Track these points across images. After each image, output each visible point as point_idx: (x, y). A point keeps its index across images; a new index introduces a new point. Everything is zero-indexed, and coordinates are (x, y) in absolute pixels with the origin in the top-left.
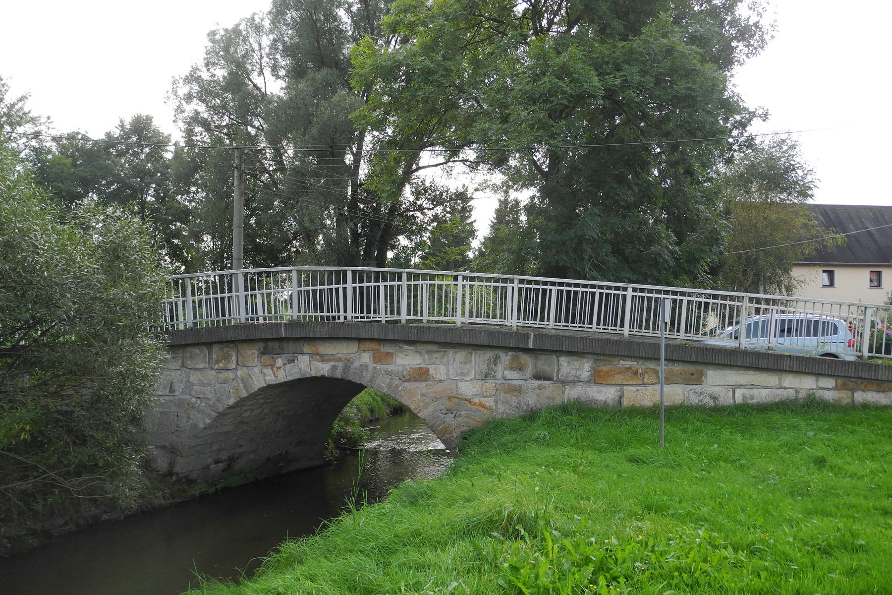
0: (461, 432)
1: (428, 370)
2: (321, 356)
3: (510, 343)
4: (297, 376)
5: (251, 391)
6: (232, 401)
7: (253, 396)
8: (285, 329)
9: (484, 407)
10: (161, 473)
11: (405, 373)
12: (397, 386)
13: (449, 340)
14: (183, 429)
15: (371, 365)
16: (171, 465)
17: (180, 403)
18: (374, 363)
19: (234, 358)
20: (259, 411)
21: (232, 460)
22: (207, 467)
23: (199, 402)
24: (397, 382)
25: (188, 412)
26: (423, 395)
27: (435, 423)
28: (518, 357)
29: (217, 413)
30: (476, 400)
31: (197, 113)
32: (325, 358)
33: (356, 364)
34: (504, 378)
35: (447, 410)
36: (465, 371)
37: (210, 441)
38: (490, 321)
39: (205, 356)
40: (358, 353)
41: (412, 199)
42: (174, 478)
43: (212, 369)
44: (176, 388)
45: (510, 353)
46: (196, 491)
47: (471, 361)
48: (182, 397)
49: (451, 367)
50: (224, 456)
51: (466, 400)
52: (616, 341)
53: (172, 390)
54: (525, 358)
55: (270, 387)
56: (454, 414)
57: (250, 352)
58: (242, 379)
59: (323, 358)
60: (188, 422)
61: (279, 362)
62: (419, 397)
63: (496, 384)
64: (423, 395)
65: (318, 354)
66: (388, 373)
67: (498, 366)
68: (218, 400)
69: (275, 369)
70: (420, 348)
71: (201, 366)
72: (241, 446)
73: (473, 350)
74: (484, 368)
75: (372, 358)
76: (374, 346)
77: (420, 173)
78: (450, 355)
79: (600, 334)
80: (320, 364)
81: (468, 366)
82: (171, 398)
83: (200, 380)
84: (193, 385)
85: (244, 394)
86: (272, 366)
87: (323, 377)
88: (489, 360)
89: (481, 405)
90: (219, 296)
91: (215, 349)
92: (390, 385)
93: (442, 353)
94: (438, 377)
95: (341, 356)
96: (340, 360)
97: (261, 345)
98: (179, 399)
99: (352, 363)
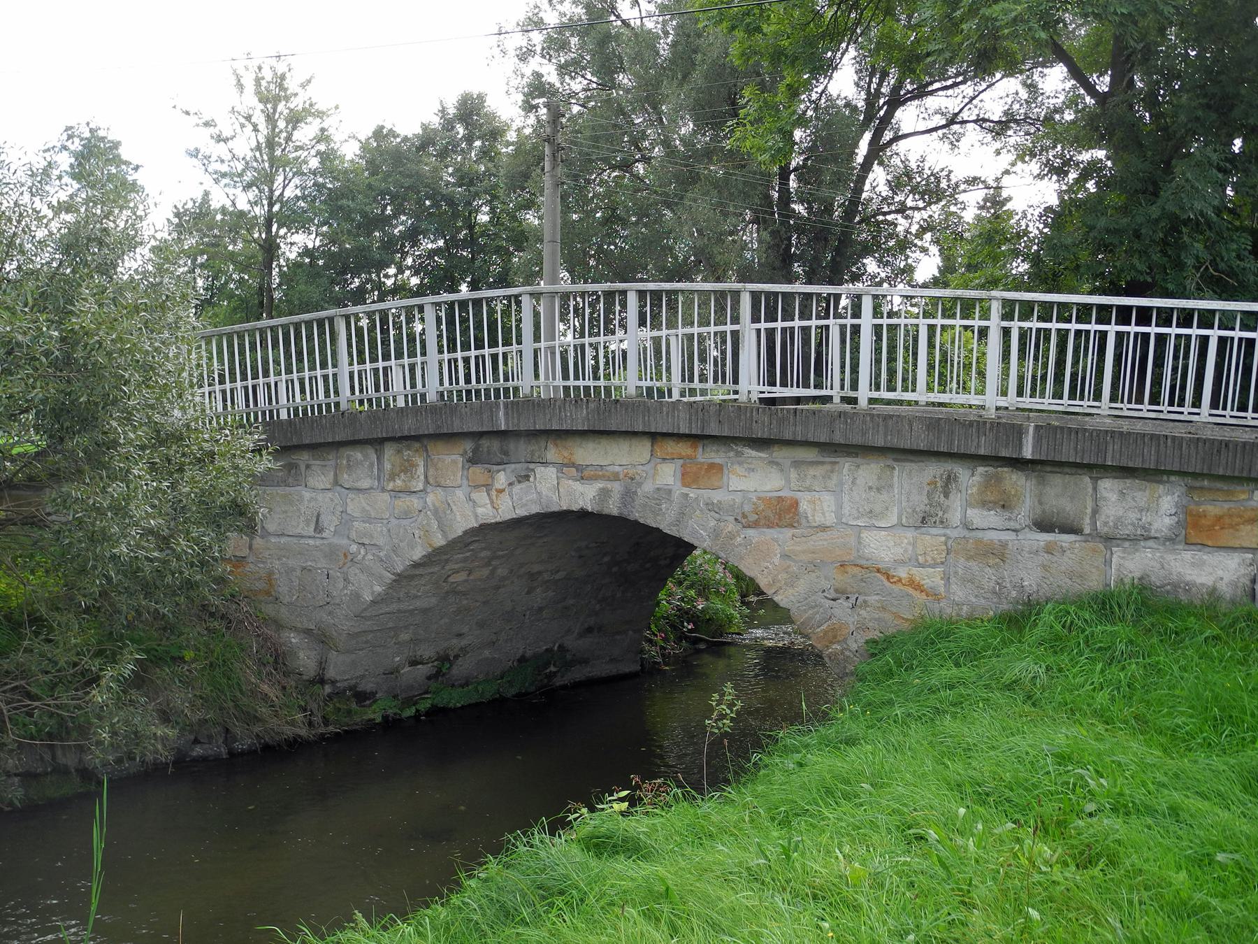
0: (867, 642)
1: (795, 504)
2: (579, 468)
3: (978, 446)
4: (535, 509)
5: (452, 536)
6: (418, 554)
7: (456, 545)
8: (506, 414)
9: (919, 587)
10: (305, 677)
11: (747, 508)
12: (731, 536)
13: (838, 438)
14: (337, 601)
15: (678, 490)
16: (322, 665)
17: (332, 553)
18: (684, 485)
19: (421, 470)
20: (486, 572)
21: (444, 659)
22: (394, 672)
23: (362, 552)
24: (731, 527)
25: (345, 569)
26: (785, 556)
27: (810, 619)
28: (999, 479)
29: (393, 574)
30: (902, 573)
31: (538, 76)
32: (586, 473)
33: (648, 487)
34: (967, 526)
35: (836, 591)
36: (878, 508)
37: (391, 625)
38: (961, 398)
39: (372, 465)
40: (652, 464)
41: (884, 190)
42: (328, 689)
43: (383, 490)
44: (325, 525)
45: (981, 470)
46: (374, 713)
47: (891, 486)
48: (335, 540)
49: (846, 498)
50: (427, 652)
51: (878, 571)
52: (1245, 444)
53: (319, 529)
54: (1015, 480)
55: (484, 529)
56: (852, 600)
57: (448, 459)
58: (436, 512)
59: (584, 474)
60: (345, 588)
61: (501, 479)
62: (777, 560)
63: (948, 538)
64: (785, 556)
65: (573, 465)
66: (712, 507)
67: (952, 496)
68: (395, 549)
69: (494, 493)
70: (781, 454)
71: (365, 484)
72: (460, 635)
73: (895, 460)
74: (920, 501)
75: (679, 475)
76: (683, 448)
77: (902, 146)
78: (845, 471)
79: (1217, 428)
80: (578, 487)
81: (884, 496)
82: (318, 542)
83: (364, 510)
84: (353, 519)
85: (439, 541)
86: (488, 487)
87: (583, 514)
88: (933, 483)
89: (912, 583)
90: (473, 353)
91: (389, 451)
92: (716, 534)
93: (828, 467)
94: (819, 519)
95: (617, 469)
96: (615, 477)
97: (468, 445)
98: (330, 544)
99: (640, 484)
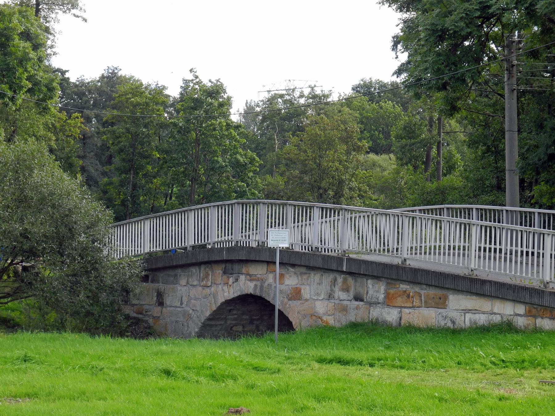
2: (250, 276)
6: (208, 314)
32: (252, 278)
45: (342, 276)
47: (322, 283)
55: (228, 302)
57: (218, 272)
60: (187, 330)
69: (229, 287)
91: (203, 267)
93: (308, 275)
97: (223, 266)
